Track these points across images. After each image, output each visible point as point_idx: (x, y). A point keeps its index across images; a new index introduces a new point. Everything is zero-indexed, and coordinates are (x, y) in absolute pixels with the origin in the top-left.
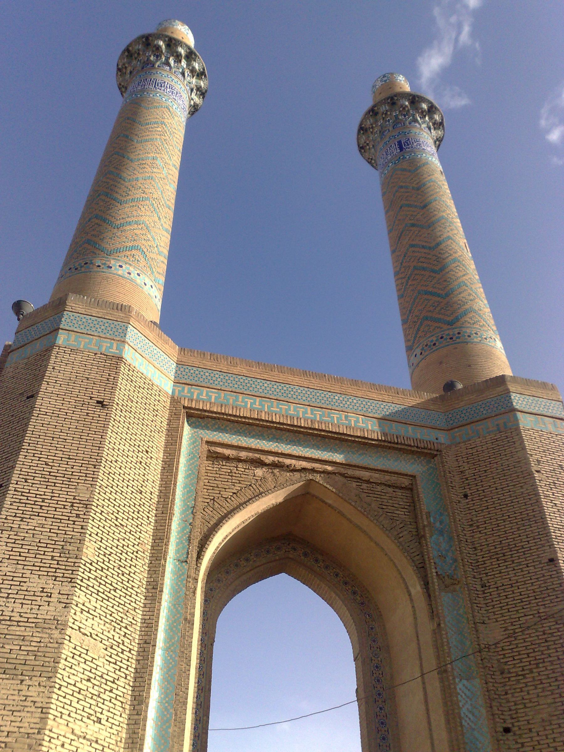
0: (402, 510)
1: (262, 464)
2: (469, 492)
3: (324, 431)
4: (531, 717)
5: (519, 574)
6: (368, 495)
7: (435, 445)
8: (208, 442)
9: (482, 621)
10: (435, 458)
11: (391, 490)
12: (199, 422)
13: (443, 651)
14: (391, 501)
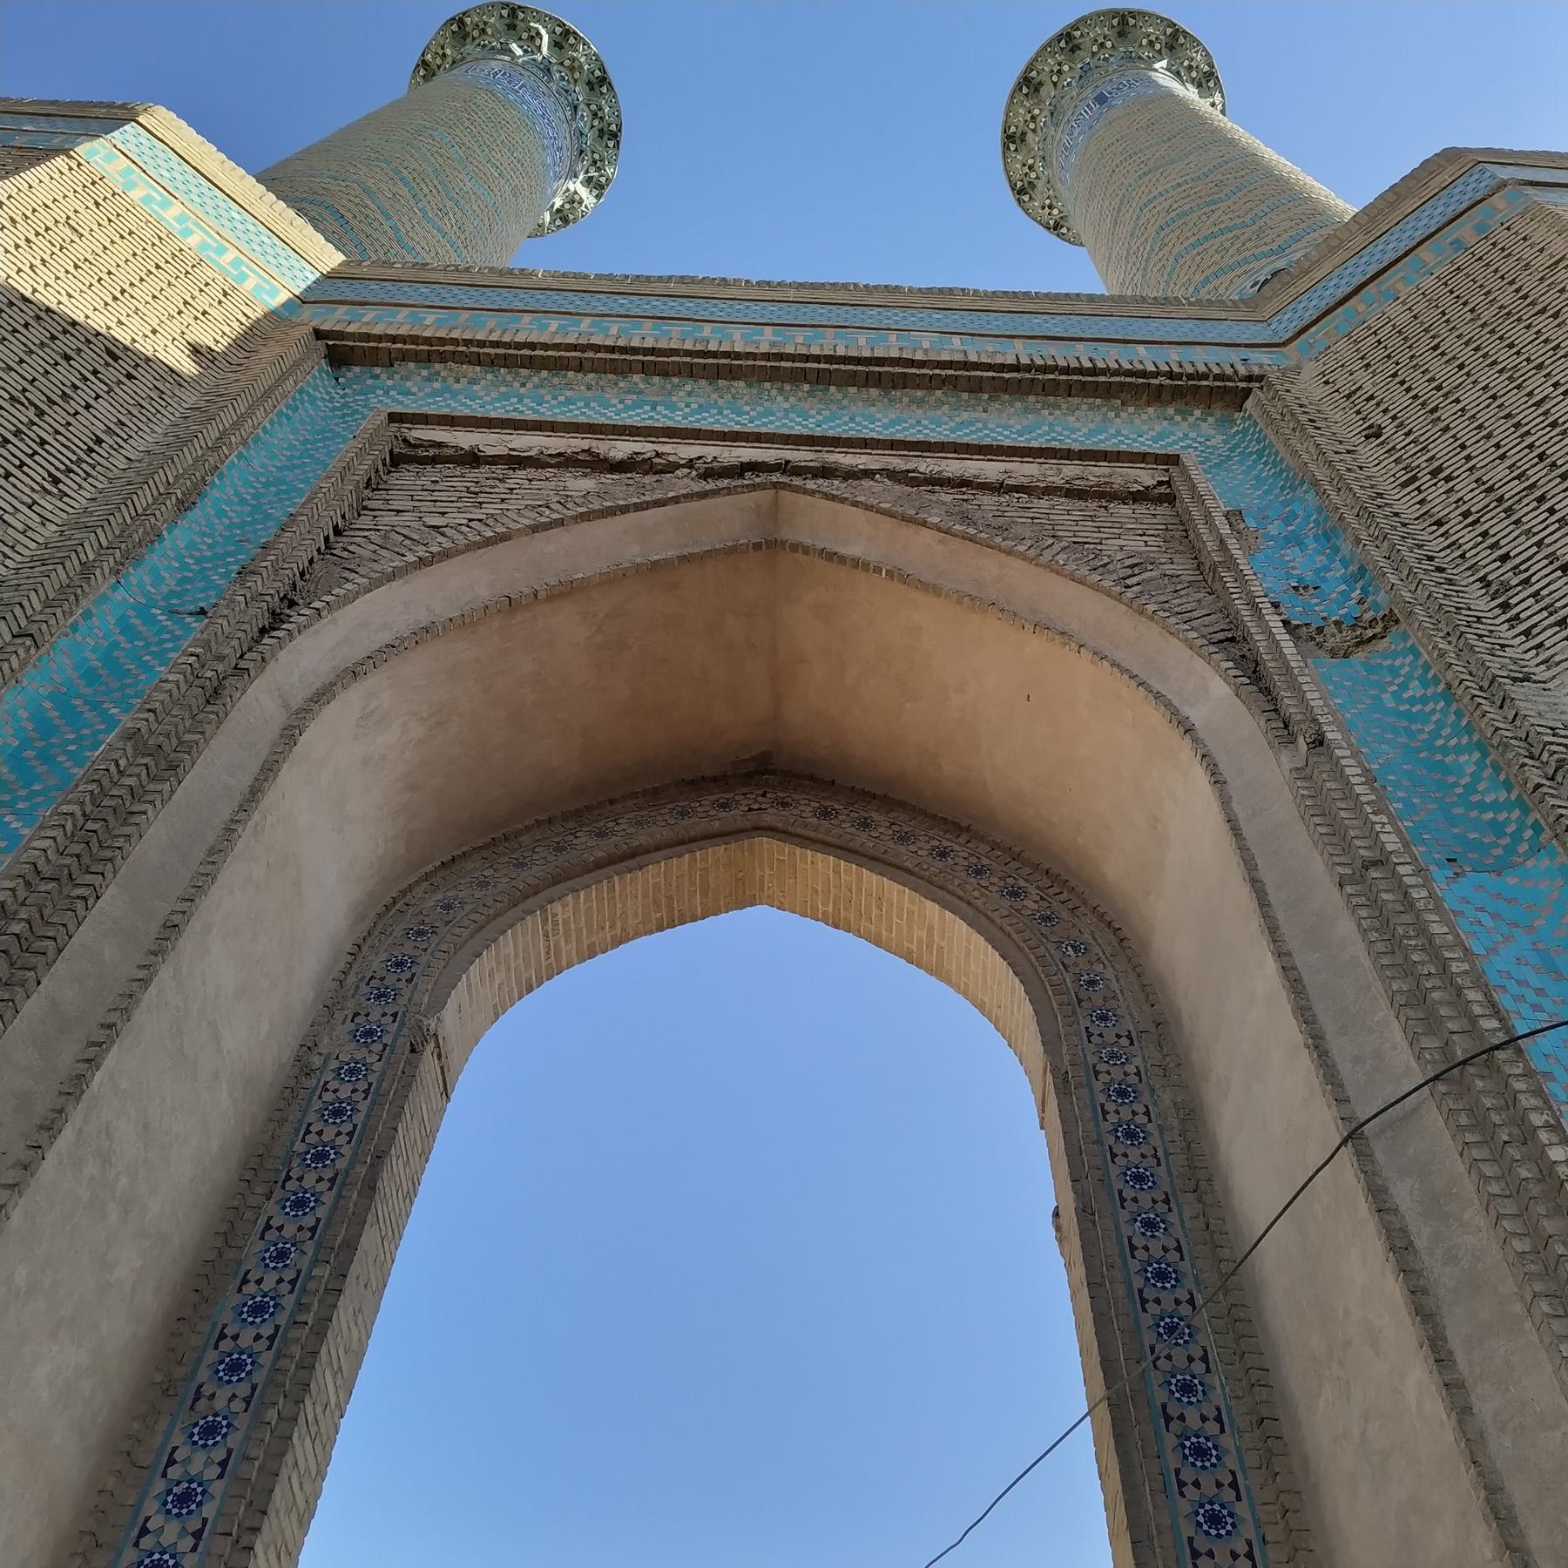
1: (597, 464)
2: (1383, 420)
10: (1248, 404)
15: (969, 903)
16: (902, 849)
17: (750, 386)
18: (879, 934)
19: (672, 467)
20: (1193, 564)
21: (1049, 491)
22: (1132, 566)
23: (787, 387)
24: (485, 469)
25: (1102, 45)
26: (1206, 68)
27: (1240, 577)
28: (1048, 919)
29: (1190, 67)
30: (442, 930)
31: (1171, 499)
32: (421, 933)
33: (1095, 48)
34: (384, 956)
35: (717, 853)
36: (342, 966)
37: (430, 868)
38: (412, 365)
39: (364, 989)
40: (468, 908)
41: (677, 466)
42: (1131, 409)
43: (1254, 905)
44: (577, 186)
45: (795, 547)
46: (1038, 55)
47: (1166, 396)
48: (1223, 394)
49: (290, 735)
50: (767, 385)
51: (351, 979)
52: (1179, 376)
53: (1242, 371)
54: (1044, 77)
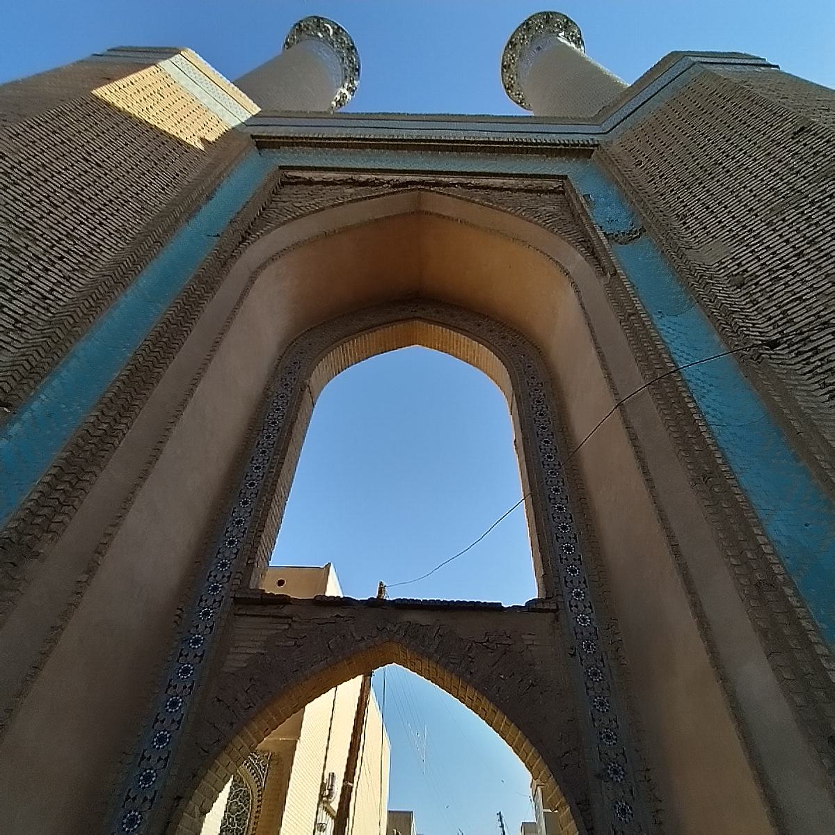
1: (355, 183)
15: (488, 341)
16: (464, 324)
18: (457, 354)
20: (570, 215)
21: (520, 190)
25: (540, 27)
26: (579, 36)
27: (588, 218)
29: (572, 36)
31: (563, 193)
35: (401, 326)
36: (276, 363)
37: (303, 331)
38: (286, 147)
39: (284, 371)
43: (589, 332)
44: (344, 91)
45: (427, 213)
48: (581, 152)
49: (252, 280)
50: (415, 152)
52: (568, 145)
53: (591, 142)
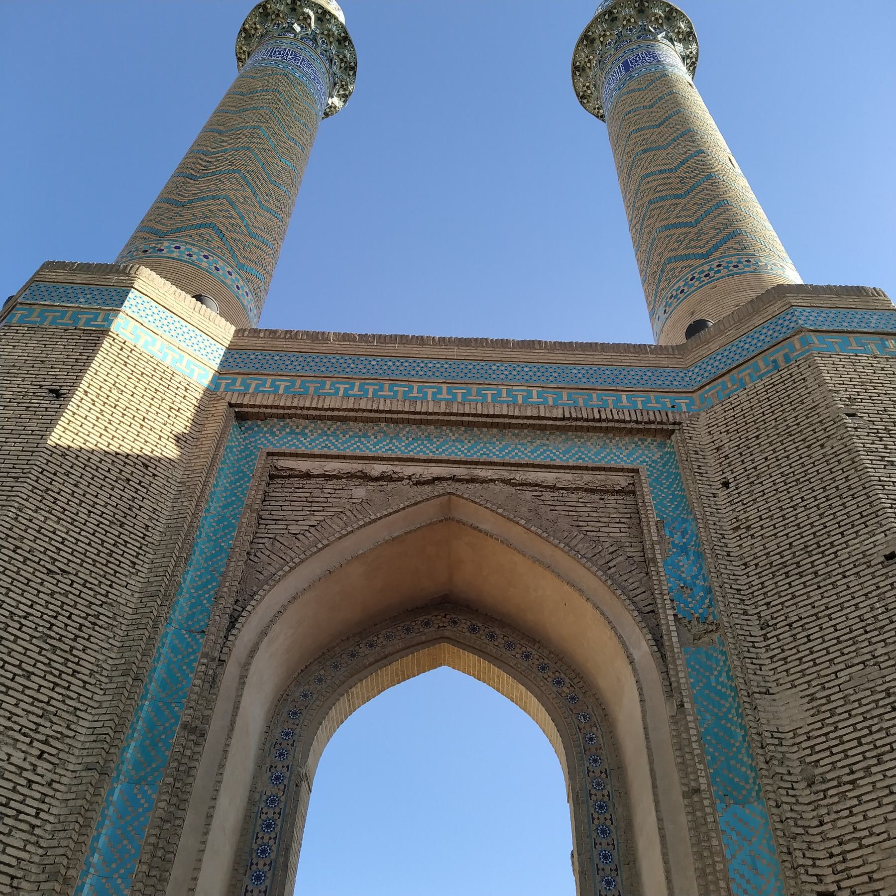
0: (617, 525)
1: (366, 478)
2: (730, 477)
3: (468, 415)
4: (874, 867)
5: (830, 593)
6: (552, 508)
7: (670, 415)
8: (269, 454)
9: (764, 690)
10: (673, 437)
11: (596, 497)
12: (259, 426)
13: (691, 753)
14: (595, 514)
16: (508, 653)
17: (436, 428)
19: (401, 479)
22: (611, 553)
23: (454, 429)
24: (313, 481)
25: (629, 21)
28: (573, 699)
29: (679, 32)
30: (304, 712)
32: (295, 714)
33: (625, 23)
34: (280, 730)
38: (275, 420)
39: (273, 751)
40: (315, 696)
41: (403, 479)
42: (617, 438)
46: (592, 22)
47: (634, 432)
48: (660, 431)
50: (445, 428)
51: (267, 745)
52: (641, 423)
54: (596, 35)
